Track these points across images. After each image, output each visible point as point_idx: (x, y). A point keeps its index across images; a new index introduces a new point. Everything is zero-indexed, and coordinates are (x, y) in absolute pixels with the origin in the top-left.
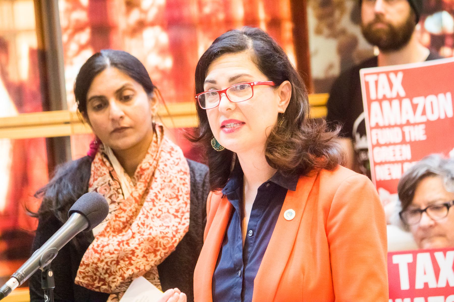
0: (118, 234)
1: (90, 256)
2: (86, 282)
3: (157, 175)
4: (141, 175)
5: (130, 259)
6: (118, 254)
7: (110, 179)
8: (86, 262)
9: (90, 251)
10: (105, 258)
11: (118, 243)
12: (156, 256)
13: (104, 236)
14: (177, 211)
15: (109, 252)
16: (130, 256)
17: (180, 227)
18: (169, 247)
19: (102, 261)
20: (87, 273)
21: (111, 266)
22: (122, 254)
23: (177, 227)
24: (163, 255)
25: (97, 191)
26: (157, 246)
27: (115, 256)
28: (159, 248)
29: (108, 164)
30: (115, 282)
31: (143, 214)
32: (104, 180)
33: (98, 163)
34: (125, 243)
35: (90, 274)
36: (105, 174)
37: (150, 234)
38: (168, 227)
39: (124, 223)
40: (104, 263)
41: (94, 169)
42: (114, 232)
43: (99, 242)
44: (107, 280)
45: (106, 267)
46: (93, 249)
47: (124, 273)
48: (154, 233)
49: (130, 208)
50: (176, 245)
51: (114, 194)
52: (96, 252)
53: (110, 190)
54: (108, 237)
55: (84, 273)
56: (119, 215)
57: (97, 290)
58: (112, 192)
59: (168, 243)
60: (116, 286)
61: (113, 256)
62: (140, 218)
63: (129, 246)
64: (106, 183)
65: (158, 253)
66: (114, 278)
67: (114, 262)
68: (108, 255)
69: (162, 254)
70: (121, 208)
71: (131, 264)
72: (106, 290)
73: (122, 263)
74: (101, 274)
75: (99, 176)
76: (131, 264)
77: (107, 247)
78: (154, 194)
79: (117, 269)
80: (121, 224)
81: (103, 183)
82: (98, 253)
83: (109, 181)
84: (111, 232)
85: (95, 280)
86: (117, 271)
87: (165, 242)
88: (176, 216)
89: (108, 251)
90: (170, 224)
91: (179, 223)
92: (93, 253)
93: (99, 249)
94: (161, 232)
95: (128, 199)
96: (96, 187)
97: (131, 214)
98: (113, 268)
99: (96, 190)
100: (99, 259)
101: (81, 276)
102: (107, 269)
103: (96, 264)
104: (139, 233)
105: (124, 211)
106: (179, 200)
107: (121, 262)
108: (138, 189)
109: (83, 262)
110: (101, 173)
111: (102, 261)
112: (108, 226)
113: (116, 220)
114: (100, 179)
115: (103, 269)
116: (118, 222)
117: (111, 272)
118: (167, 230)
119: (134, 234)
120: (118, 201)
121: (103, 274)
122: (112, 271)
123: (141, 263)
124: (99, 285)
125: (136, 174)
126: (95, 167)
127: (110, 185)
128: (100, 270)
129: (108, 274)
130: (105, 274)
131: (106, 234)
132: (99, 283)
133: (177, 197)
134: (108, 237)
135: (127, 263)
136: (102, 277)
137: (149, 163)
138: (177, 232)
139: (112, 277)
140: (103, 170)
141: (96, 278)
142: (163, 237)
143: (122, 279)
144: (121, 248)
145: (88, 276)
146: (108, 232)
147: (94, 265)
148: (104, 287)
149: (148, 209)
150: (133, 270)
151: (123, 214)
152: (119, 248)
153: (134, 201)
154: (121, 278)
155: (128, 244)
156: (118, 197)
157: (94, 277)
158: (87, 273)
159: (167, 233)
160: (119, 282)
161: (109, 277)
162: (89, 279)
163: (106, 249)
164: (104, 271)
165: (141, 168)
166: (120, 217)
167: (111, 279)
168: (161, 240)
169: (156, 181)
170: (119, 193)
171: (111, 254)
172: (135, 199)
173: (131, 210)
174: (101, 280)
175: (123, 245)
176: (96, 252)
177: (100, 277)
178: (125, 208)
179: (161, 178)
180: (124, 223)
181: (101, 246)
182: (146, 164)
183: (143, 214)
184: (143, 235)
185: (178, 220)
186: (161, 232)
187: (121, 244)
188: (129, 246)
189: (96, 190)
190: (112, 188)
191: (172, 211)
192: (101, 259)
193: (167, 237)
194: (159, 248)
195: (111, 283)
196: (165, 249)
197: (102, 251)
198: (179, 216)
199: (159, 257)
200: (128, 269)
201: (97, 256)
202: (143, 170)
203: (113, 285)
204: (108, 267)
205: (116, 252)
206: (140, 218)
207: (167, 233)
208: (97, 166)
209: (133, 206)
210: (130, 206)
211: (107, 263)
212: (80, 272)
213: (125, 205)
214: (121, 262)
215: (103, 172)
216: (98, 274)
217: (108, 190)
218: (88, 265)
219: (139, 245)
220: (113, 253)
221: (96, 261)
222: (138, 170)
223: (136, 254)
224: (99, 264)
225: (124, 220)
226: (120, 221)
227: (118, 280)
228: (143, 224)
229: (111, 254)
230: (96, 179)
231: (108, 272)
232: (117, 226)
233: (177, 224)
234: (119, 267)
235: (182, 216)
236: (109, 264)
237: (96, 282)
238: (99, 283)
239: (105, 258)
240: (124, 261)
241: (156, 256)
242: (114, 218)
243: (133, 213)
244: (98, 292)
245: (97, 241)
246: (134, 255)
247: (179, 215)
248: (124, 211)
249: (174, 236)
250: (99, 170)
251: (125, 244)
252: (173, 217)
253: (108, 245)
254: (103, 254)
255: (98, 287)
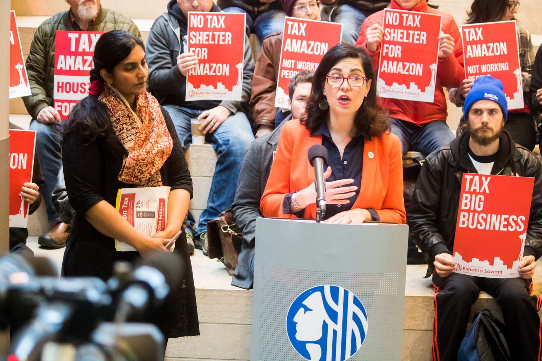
0: (141, 148)
1: (130, 162)
2: (128, 178)
3: (152, 110)
4: (140, 110)
5: (153, 163)
6: (147, 160)
7: (129, 113)
8: (129, 166)
9: (129, 159)
10: (140, 163)
11: (146, 153)
12: (163, 160)
13: (135, 150)
14: (165, 132)
15: (142, 159)
16: (153, 161)
17: (170, 141)
18: (168, 154)
19: (138, 164)
20: (129, 173)
21: (143, 168)
22: (149, 160)
23: (168, 142)
24: (166, 159)
25: (120, 121)
26: (163, 154)
27: (146, 161)
28: (164, 155)
29: (122, 103)
30: (145, 177)
31: (156, 135)
32: (124, 113)
33: (115, 102)
34: (151, 153)
35: (131, 173)
36: (124, 110)
37: (161, 147)
38: (165, 142)
39: (143, 141)
40: (138, 166)
41: (111, 106)
42: (139, 147)
43: (133, 154)
44: (139, 177)
45: (140, 168)
46: (130, 157)
47: (151, 171)
48: (163, 146)
49: (145, 132)
50: (171, 152)
51: (132, 123)
52: (134, 160)
53: (130, 120)
54: (137, 151)
55: (127, 173)
56: (140, 137)
57: (132, 183)
58: (131, 121)
59: (168, 152)
60: (145, 180)
61: (144, 161)
62: (155, 137)
63: (153, 155)
64: (125, 115)
65: (164, 158)
66: (144, 175)
67: (145, 165)
68: (141, 161)
69: (166, 158)
70: (140, 132)
71: (154, 166)
72: (137, 183)
73: (149, 166)
74: (136, 173)
75: (119, 111)
76: (154, 166)
77: (140, 156)
78: (157, 122)
79: (146, 170)
80: (142, 142)
81: (123, 115)
82: (135, 160)
83: (128, 114)
84: (137, 147)
85: (131, 177)
86: (146, 171)
87: (167, 151)
88: (165, 136)
89: (141, 158)
90: (165, 140)
91: (169, 140)
92: (132, 160)
93: (136, 158)
94: (165, 145)
95: (143, 126)
96: (119, 117)
97: (146, 136)
98: (144, 169)
99: (119, 119)
100: (136, 164)
101: (125, 175)
102: (140, 170)
103: (134, 167)
104: (155, 146)
105: (142, 134)
106: (163, 125)
107: (149, 165)
108: (147, 120)
109: (126, 166)
110: (120, 109)
111: (138, 164)
112: (135, 144)
113: (139, 140)
114: (120, 112)
115: (138, 169)
116: (139, 141)
117: (142, 171)
118: (166, 144)
119: (153, 147)
120: (135, 127)
121: (137, 173)
122: (143, 171)
123: (159, 164)
124: (134, 180)
125: (137, 109)
126: (112, 104)
127: (129, 117)
128: (136, 170)
129: (140, 173)
130: (138, 173)
131: (136, 149)
132: (134, 179)
133: (162, 123)
134: (137, 151)
135: (151, 165)
136: (136, 175)
137: (143, 102)
138: (170, 143)
139: (143, 174)
140: (121, 107)
141: (133, 175)
142: (166, 148)
143: (150, 175)
144: (149, 157)
145: (129, 175)
146: (136, 147)
147: (133, 168)
148: (136, 181)
149: (157, 131)
150: (156, 169)
151: (141, 136)
152: (148, 157)
153: (146, 128)
154: (149, 175)
155: (152, 154)
156: (135, 125)
157: (132, 175)
158: (129, 173)
159: (167, 145)
160: (148, 178)
161: (141, 175)
162: (129, 176)
163: (140, 157)
164: (138, 171)
165: (139, 105)
166: (141, 138)
167: (142, 176)
168: (165, 150)
169: (154, 114)
170: (135, 122)
171: (143, 160)
172: (147, 126)
173: (145, 133)
174: (135, 177)
175: (150, 155)
176: (134, 160)
177: (135, 175)
178: (142, 132)
179: (154, 111)
180: (143, 141)
181: (136, 156)
182: (141, 103)
183: (156, 135)
184: (157, 148)
185: (167, 138)
186: (165, 145)
187: (149, 154)
188: (153, 155)
189: (119, 119)
190: (131, 119)
191: (163, 132)
192: (137, 164)
193: (167, 148)
194: (163, 155)
195: (141, 178)
196: (166, 155)
197: (138, 159)
198: (167, 135)
199: (164, 161)
200: (152, 169)
201: (135, 162)
202: (141, 107)
203: (143, 180)
204: (141, 168)
205: (146, 159)
206: (155, 137)
207: (167, 145)
208: (113, 104)
209: (146, 130)
210: (145, 130)
211: (140, 166)
212: (125, 173)
213: (142, 130)
214: (149, 165)
215: (122, 109)
216: (134, 173)
217: (128, 120)
218: (130, 168)
219: (157, 154)
220: (145, 160)
221: (134, 165)
222: (138, 107)
223: (155, 159)
224: (136, 167)
225: (142, 139)
226: (141, 140)
227: (147, 176)
228: (156, 141)
229: (143, 160)
230: (117, 113)
231: (140, 171)
232: (140, 143)
233: (168, 140)
234: (147, 168)
235: (168, 135)
236: (142, 166)
237: (132, 178)
238: (134, 179)
239: (140, 163)
240: (150, 164)
241: (163, 160)
242: (137, 138)
243: (147, 134)
244: (131, 184)
245: (131, 154)
246: (155, 160)
247: (166, 134)
248: (142, 134)
249: (170, 147)
250: (117, 107)
251: (151, 154)
252: (164, 136)
253: (140, 155)
254: (139, 161)
255: (133, 181)
